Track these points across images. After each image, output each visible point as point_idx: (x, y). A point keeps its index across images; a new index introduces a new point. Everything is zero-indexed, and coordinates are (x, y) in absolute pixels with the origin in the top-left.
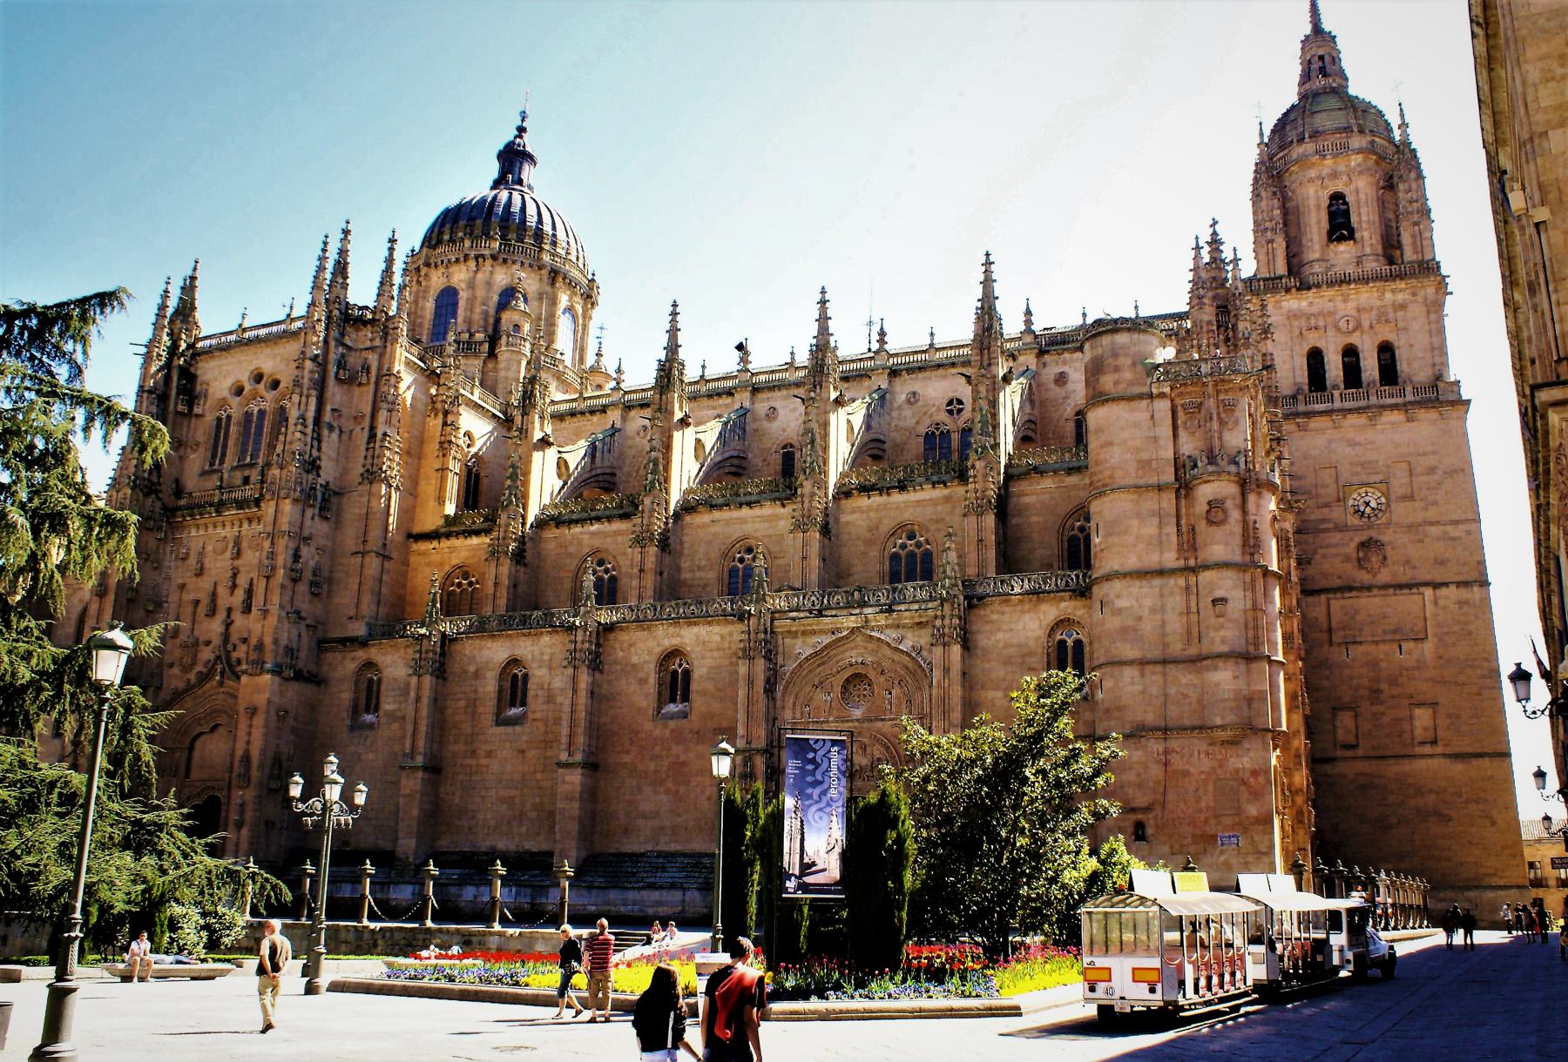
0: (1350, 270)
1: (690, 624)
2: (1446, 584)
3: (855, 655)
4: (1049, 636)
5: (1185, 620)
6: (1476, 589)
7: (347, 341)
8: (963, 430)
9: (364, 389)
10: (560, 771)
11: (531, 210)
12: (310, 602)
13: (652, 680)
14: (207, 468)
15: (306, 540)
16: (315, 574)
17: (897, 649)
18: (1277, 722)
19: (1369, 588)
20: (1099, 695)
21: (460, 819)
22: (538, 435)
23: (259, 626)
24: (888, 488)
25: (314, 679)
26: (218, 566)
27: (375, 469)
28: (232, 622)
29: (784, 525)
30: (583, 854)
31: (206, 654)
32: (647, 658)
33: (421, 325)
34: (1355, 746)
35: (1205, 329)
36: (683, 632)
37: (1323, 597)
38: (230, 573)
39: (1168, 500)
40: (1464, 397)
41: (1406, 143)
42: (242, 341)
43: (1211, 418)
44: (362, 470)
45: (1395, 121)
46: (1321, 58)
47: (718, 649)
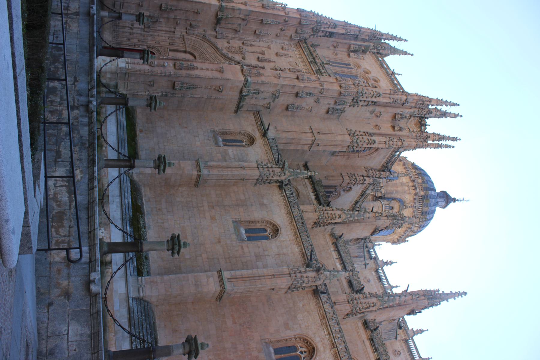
7: (412, 118)
9: (391, 129)
10: (216, 273)
12: (283, 105)
13: (289, 334)
15: (317, 101)
16: (298, 106)
21: (166, 202)
23: (270, 74)
30: (153, 300)
31: (238, 58)
36: (328, 351)
38: (282, 68)
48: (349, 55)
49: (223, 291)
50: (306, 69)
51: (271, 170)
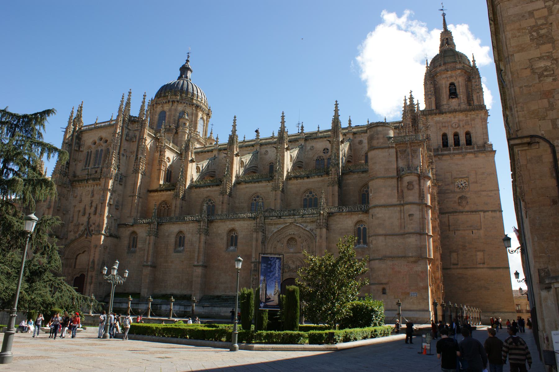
0: (456, 108)
1: (238, 220)
2: (488, 211)
3: (291, 231)
4: (355, 226)
5: (400, 221)
6: (498, 213)
7: (129, 127)
8: (329, 159)
9: (135, 143)
10: (194, 268)
11: (190, 87)
13: (225, 238)
14: (84, 168)
16: (117, 203)
17: (305, 230)
18: (430, 255)
19: (462, 212)
20: (371, 246)
22: (190, 159)
23: (99, 219)
24: (303, 177)
25: (116, 237)
26: (86, 200)
27: (137, 169)
28: (90, 218)
29: (269, 189)
31: (82, 228)
32: (223, 231)
33: (154, 123)
34: (457, 264)
35: (408, 126)
36: (235, 223)
37: (447, 215)
38: (90, 202)
39: (394, 182)
40: (494, 150)
41: (474, 66)
42: (96, 127)
43: (409, 155)
44: (133, 169)
45: (471, 60)
46: (447, 39)
47: (247, 229)
48: (81, 151)
49: (202, 266)
50: (91, 186)
51: (151, 229)
